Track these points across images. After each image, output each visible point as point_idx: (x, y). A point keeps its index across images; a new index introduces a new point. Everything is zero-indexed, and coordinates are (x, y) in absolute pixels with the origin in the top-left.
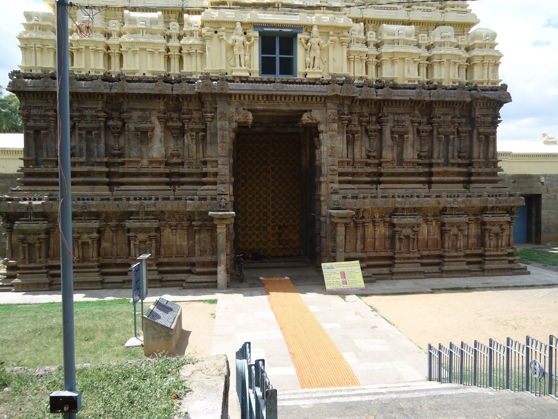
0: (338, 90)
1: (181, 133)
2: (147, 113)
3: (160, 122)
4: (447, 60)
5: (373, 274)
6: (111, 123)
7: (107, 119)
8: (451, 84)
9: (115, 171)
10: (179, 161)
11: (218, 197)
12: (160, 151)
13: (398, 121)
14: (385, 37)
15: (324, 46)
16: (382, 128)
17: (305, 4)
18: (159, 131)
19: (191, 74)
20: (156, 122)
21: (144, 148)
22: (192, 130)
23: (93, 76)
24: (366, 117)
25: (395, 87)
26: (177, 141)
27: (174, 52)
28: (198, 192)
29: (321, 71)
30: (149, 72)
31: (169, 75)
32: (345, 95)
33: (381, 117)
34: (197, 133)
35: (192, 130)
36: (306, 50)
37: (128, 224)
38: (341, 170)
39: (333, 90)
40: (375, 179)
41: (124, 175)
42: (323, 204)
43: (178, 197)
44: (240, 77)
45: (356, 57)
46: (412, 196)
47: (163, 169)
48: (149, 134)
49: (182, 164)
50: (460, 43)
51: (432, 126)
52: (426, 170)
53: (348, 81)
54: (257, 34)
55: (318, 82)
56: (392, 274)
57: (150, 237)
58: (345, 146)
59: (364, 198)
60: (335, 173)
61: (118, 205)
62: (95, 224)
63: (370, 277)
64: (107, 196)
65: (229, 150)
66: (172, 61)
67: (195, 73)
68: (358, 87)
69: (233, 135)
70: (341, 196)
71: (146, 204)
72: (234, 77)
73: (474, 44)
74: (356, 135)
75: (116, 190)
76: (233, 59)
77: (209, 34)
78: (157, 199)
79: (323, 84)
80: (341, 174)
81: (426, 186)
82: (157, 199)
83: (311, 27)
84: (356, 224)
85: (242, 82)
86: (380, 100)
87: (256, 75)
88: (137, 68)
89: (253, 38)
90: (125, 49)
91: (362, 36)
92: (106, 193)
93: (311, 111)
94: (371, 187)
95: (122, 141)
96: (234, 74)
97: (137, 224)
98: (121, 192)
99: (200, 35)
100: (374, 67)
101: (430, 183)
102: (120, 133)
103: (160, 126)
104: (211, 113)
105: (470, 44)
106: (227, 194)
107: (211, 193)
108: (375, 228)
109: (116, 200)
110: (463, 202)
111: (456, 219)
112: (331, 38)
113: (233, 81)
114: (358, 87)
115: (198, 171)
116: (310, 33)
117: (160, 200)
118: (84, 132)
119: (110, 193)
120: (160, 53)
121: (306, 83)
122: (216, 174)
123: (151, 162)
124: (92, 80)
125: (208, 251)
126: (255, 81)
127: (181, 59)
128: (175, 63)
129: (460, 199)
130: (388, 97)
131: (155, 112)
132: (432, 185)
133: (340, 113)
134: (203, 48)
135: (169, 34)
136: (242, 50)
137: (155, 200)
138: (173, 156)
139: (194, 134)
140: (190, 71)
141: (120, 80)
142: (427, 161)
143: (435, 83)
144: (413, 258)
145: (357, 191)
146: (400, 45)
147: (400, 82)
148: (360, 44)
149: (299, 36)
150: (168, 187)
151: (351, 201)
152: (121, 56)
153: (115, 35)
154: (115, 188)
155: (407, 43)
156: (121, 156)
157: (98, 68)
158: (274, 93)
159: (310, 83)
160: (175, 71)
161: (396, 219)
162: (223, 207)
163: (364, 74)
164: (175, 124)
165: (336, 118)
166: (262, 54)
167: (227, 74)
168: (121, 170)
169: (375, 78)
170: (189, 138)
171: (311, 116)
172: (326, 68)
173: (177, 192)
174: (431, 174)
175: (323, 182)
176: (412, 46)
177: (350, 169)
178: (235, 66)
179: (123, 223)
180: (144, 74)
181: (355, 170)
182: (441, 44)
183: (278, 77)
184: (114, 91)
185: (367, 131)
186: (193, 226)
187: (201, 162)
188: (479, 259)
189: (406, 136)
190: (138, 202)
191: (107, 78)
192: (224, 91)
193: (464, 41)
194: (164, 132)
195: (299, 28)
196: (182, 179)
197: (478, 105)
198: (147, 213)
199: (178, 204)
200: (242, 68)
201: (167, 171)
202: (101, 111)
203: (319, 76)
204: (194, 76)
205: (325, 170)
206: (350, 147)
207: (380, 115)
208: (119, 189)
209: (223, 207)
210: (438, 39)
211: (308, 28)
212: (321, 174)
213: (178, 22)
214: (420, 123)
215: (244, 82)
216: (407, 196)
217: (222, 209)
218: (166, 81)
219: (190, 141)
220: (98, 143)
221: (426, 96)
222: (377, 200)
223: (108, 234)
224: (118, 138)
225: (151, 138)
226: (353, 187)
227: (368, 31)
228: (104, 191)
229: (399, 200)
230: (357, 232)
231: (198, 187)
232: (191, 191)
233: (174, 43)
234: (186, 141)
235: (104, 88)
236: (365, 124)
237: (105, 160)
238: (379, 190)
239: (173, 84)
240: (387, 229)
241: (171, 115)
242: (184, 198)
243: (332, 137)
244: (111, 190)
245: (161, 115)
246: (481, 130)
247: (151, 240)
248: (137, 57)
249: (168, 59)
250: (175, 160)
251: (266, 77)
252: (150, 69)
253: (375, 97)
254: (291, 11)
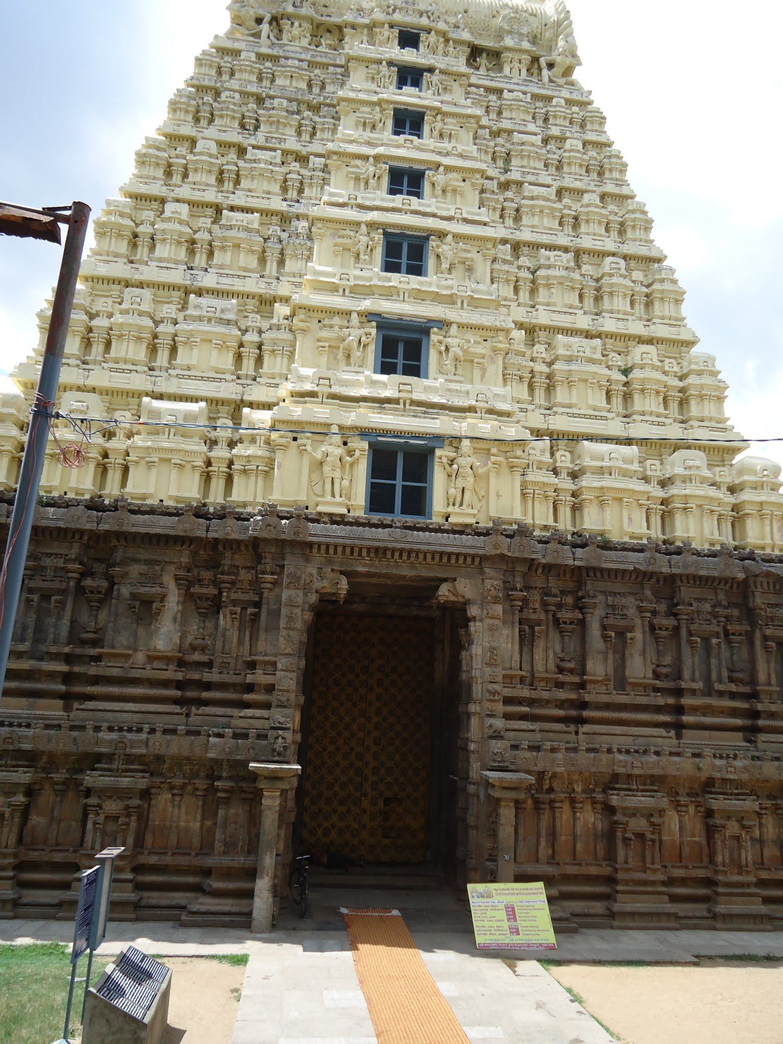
0: (504, 546)
1: (215, 606)
2: (157, 568)
3: (178, 585)
4: (697, 505)
5: (574, 915)
6: (88, 582)
7: (83, 575)
8: (707, 546)
9: (82, 671)
10: (205, 658)
11: (271, 733)
12: (171, 639)
13: (613, 607)
14: (587, 462)
15: (480, 471)
16: (584, 618)
17: (450, 403)
18: (173, 601)
19: (245, 505)
20: (172, 585)
21: (141, 631)
22: (234, 603)
23: (71, 500)
24: (555, 596)
25: (607, 546)
26: (204, 621)
27: (219, 468)
28: (234, 722)
29: (475, 511)
30: (170, 497)
31: (205, 505)
32: (516, 555)
33: (583, 597)
34: (244, 609)
35: (234, 603)
36: (449, 476)
37: (90, 779)
38: (508, 692)
39: (496, 547)
40: (573, 713)
41: (96, 680)
42: (473, 757)
43: (193, 728)
44: (331, 515)
45: (537, 492)
46: (645, 752)
47: (172, 673)
48: (154, 605)
49: (209, 665)
50: (718, 479)
51: (678, 620)
52: (671, 701)
53: (523, 531)
54: (365, 445)
55: (468, 531)
56: (612, 915)
57: (127, 807)
58: (517, 647)
59: (553, 750)
60: (496, 697)
61: (75, 739)
62: (24, 776)
63: (566, 919)
64: (58, 719)
65: (300, 642)
66: (214, 482)
67: (251, 503)
68: (540, 542)
69: (308, 616)
70: (508, 744)
71: (130, 740)
72: (320, 514)
73: (743, 483)
74: (537, 628)
75: (77, 709)
76: (321, 484)
77: (283, 441)
78: (152, 731)
79: (479, 534)
80: (508, 701)
82: (152, 731)
83: (459, 439)
84: (537, 802)
85: (333, 522)
86: (580, 568)
87: (359, 513)
88: (151, 490)
89: (357, 451)
90: (135, 459)
91: (547, 458)
92: (57, 713)
93: (455, 580)
94: (565, 729)
95: (103, 616)
96: (321, 509)
97: (106, 781)
98: (85, 713)
99: (268, 442)
100: (568, 510)
101: (679, 727)
102: (101, 602)
103: (177, 592)
104: (272, 574)
105: (737, 482)
106: (288, 729)
107: (258, 724)
108: (575, 813)
109: (72, 728)
110: (745, 768)
111: (735, 804)
112: (493, 459)
113: (317, 521)
114: (540, 542)
115: (238, 679)
116: (457, 448)
117: (158, 734)
118: (35, 597)
119: (65, 714)
120: (194, 467)
121: (447, 531)
122: (270, 689)
123: (151, 659)
124: (67, 506)
125: (241, 843)
126: (357, 523)
127: (229, 479)
128: (217, 484)
129: (739, 763)
130: (594, 563)
131: (172, 568)
132: (684, 731)
133: (508, 587)
134: (271, 463)
135: (213, 438)
136: (338, 470)
137: (149, 733)
138: (194, 648)
139: (238, 610)
140: (242, 499)
141: (116, 509)
142: (670, 685)
143: (679, 544)
144: (653, 883)
145: (538, 736)
146: (613, 476)
147: (615, 537)
148: (544, 471)
149: (438, 452)
150: (177, 709)
151: (528, 754)
152: (126, 469)
153: (120, 434)
154: (76, 705)
155: (625, 474)
156: (96, 643)
157: (81, 487)
158: (390, 545)
159: (455, 532)
160: (216, 497)
161: (615, 797)
162: (279, 754)
163: (551, 522)
164: (205, 591)
165: (501, 595)
166: (372, 478)
167: (307, 508)
168: (92, 670)
169: (570, 528)
170: (228, 616)
171: (455, 588)
172: (484, 508)
173: (192, 719)
174: (679, 710)
175: (474, 714)
176: (635, 479)
177: (525, 693)
178: (323, 496)
179: (79, 777)
180: (162, 501)
181: (534, 695)
182: (687, 479)
183: (398, 518)
184: (104, 527)
185: (557, 622)
186: (217, 790)
187: (245, 662)
189: (629, 635)
190: (114, 736)
191: (95, 505)
192: (300, 538)
193: (725, 476)
194: (183, 603)
195: (439, 439)
196: (205, 695)
197: (759, 586)
198: (130, 759)
199: (192, 743)
200: (335, 500)
201: (179, 676)
202: (75, 560)
203: (471, 520)
204: (249, 509)
205: (477, 690)
206: (525, 649)
207: (580, 594)
208: (82, 707)
209: (279, 754)
210: (679, 470)
211: (455, 440)
212: (469, 699)
213: (233, 419)
214: (654, 613)
215: (338, 523)
216: (637, 751)
217: (276, 759)
218: (197, 515)
219: (229, 623)
220: (59, 618)
221: (663, 565)
222: (579, 755)
223: (46, 797)
224: (97, 611)
225: (158, 614)
226: (531, 727)
227: (558, 450)
228: (53, 710)
229: (621, 757)
230: (539, 819)
231: (235, 712)
232: (220, 719)
233: (221, 453)
234: (222, 622)
235: (86, 521)
236: (553, 608)
237: (67, 650)
238: (581, 737)
239: (210, 519)
240: (600, 816)
241: (199, 574)
242: (205, 731)
243: (492, 629)
244: (67, 708)
245: (181, 573)
246: (768, 632)
247: (128, 815)
248: (154, 471)
249: (207, 478)
250: (197, 657)
251: (376, 518)
252: (173, 492)
253: (570, 562)
254: (425, 413)
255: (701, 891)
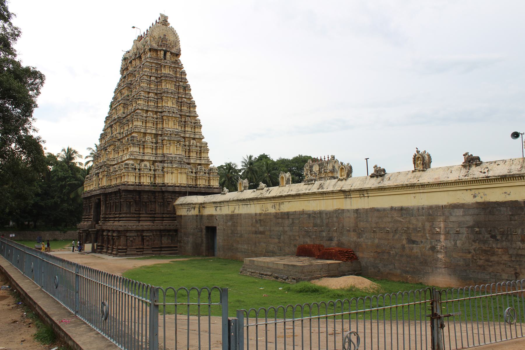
81: (138, 222)
101: (139, 221)
142: (138, 212)
143: (142, 183)
188: (142, 250)
246: (159, 201)
255: (142, 250)
